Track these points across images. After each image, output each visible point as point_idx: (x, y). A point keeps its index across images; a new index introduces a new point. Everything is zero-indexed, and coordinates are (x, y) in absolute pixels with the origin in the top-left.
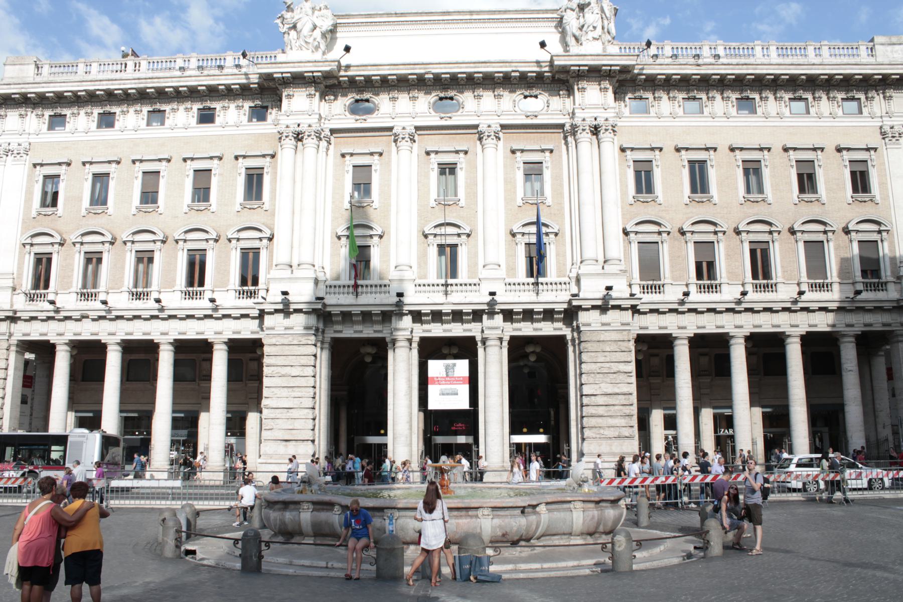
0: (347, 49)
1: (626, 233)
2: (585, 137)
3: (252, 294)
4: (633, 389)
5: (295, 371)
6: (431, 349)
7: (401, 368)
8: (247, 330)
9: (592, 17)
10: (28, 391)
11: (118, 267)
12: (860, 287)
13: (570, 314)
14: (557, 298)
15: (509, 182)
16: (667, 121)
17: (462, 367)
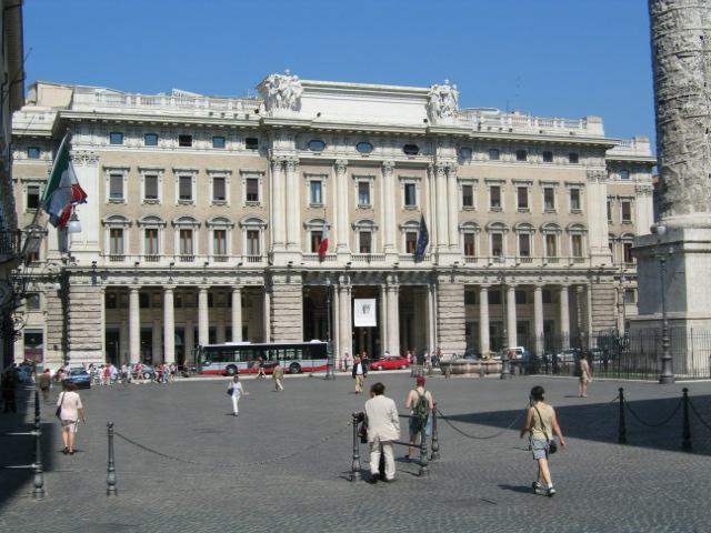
0: (319, 115)
1: (459, 229)
2: (441, 174)
3: (258, 259)
4: (463, 315)
5: (291, 306)
6: (358, 293)
7: (342, 301)
8: (258, 281)
9: (448, 102)
10: (228, 324)
11: (170, 240)
12: (572, 262)
13: (433, 275)
14: (426, 265)
15: (397, 196)
16: (481, 166)
17: (372, 302)
